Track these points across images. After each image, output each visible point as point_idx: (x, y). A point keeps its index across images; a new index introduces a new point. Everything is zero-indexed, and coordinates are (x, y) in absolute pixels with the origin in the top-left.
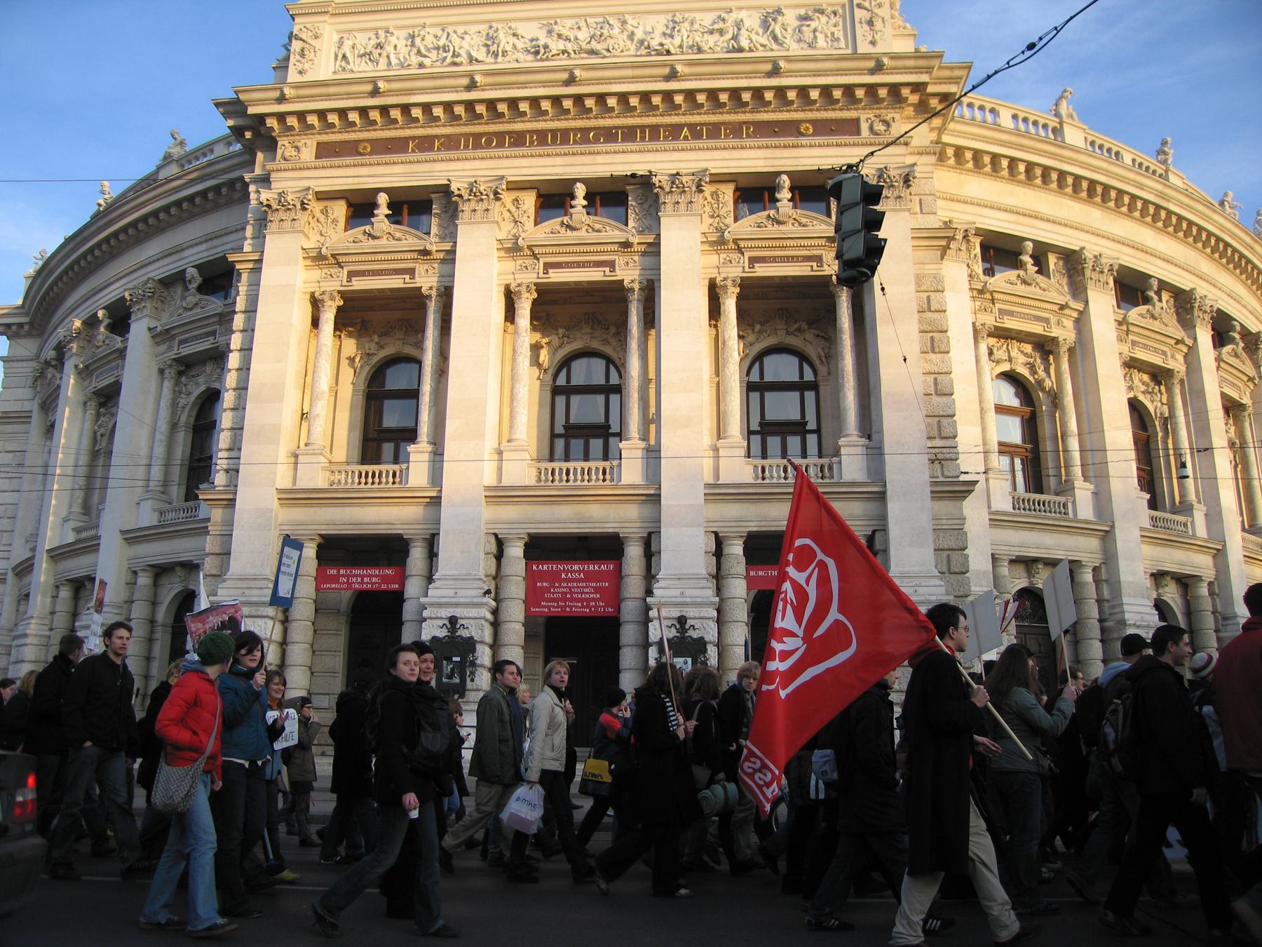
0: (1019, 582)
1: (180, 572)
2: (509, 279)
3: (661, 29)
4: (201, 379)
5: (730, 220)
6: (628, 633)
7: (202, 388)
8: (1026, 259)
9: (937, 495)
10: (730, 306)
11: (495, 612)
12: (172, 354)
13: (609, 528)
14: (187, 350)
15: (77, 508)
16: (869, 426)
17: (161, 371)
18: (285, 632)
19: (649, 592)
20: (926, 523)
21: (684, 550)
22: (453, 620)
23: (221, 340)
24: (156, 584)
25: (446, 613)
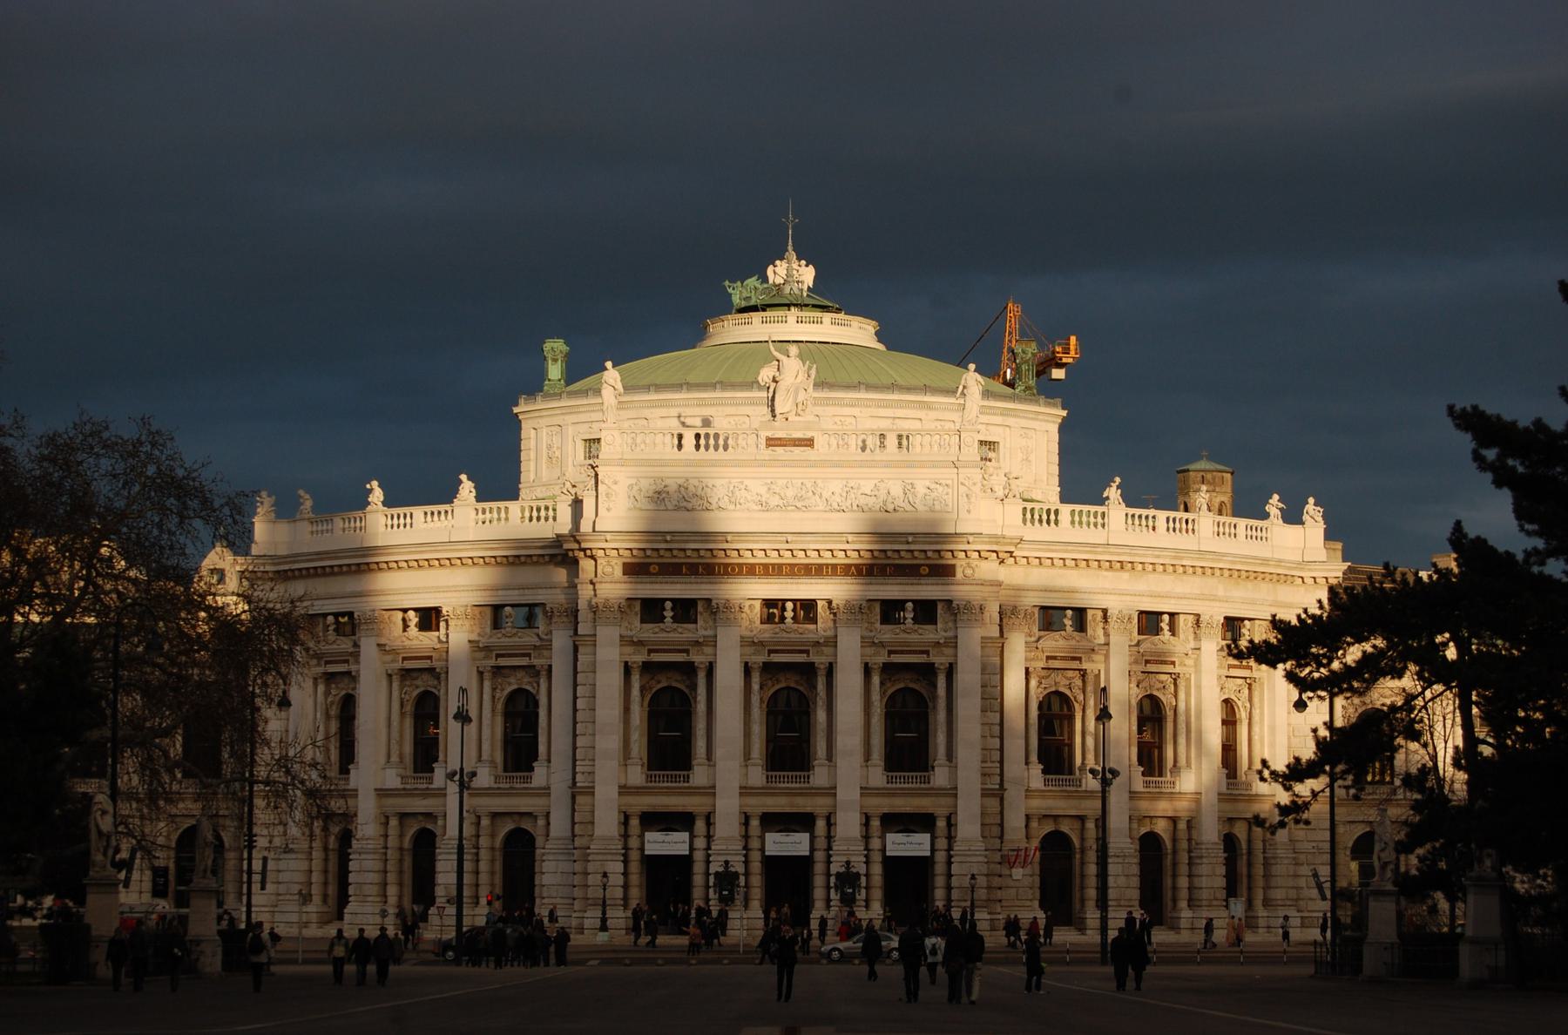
0: (1049, 827)
1: (516, 818)
2: (746, 659)
3: (838, 491)
4: (512, 680)
5: (878, 625)
6: (819, 868)
7: (515, 687)
8: (1068, 622)
9: (983, 795)
10: (876, 680)
11: (746, 856)
12: (492, 662)
13: (808, 810)
14: (503, 662)
15: (395, 758)
16: (950, 755)
17: (481, 673)
18: (626, 867)
19: (829, 848)
20: (977, 810)
21: (848, 825)
22: (727, 862)
23: (535, 662)
24: (492, 824)
25: (723, 858)
